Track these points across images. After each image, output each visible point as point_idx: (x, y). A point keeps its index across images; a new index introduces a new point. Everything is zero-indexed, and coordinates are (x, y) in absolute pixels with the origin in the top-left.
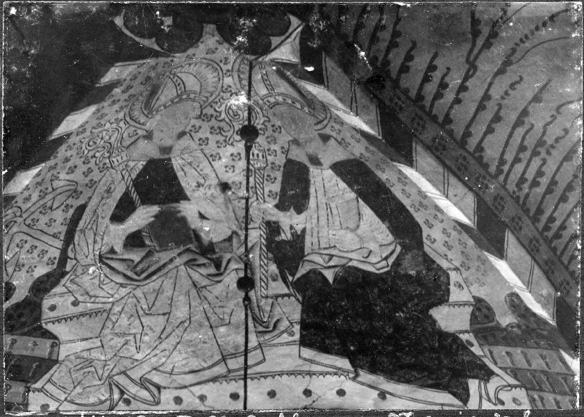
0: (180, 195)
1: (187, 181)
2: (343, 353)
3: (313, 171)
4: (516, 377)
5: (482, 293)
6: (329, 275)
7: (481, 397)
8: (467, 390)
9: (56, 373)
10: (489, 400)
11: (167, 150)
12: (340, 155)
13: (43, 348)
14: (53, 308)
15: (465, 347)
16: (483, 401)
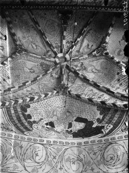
0: (55, 127)
1: (56, 126)
2: (81, 137)
3: (73, 123)
4: (107, 124)
5: (97, 118)
6: (76, 132)
7: (105, 131)
8: (102, 131)
9: (31, 132)
10: (106, 130)
11: (53, 121)
12: (75, 118)
13: (31, 129)
14: (34, 126)
15: (99, 126)
16: (106, 131)
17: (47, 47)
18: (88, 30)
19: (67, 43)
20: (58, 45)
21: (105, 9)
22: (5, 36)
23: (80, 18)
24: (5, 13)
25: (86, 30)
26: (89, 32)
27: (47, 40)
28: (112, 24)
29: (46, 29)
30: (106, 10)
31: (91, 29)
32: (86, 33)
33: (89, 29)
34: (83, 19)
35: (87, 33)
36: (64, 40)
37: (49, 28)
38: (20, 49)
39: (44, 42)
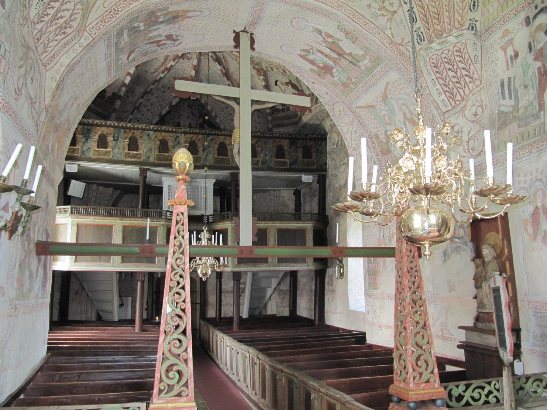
17: (222, 57)
18: (158, 72)
19: (190, 57)
20: (204, 56)
21: (149, 127)
22: (276, 84)
23: (169, 88)
24: (270, 112)
25: (160, 73)
26: (155, 69)
27: (219, 67)
28: (126, 88)
29: (219, 78)
30: (148, 126)
31: (154, 73)
32: (161, 69)
33: (156, 74)
34: (163, 87)
35: (159, 69)
36: (196, 64)
37: (215, 79)
38: (261, 71)
39: (224, 63)
